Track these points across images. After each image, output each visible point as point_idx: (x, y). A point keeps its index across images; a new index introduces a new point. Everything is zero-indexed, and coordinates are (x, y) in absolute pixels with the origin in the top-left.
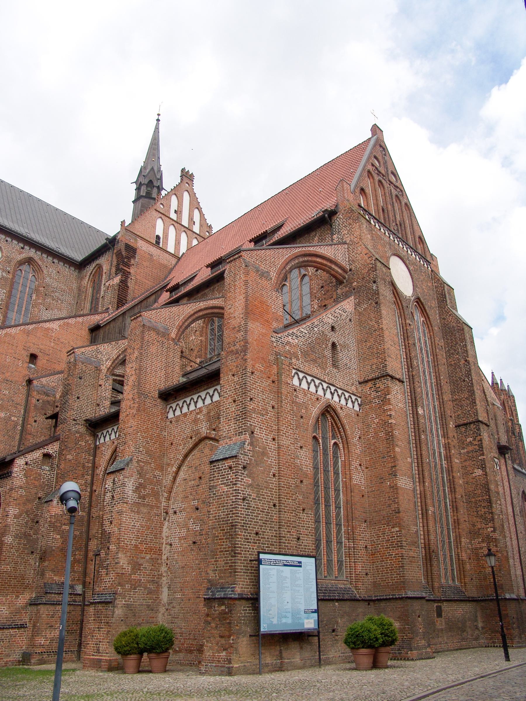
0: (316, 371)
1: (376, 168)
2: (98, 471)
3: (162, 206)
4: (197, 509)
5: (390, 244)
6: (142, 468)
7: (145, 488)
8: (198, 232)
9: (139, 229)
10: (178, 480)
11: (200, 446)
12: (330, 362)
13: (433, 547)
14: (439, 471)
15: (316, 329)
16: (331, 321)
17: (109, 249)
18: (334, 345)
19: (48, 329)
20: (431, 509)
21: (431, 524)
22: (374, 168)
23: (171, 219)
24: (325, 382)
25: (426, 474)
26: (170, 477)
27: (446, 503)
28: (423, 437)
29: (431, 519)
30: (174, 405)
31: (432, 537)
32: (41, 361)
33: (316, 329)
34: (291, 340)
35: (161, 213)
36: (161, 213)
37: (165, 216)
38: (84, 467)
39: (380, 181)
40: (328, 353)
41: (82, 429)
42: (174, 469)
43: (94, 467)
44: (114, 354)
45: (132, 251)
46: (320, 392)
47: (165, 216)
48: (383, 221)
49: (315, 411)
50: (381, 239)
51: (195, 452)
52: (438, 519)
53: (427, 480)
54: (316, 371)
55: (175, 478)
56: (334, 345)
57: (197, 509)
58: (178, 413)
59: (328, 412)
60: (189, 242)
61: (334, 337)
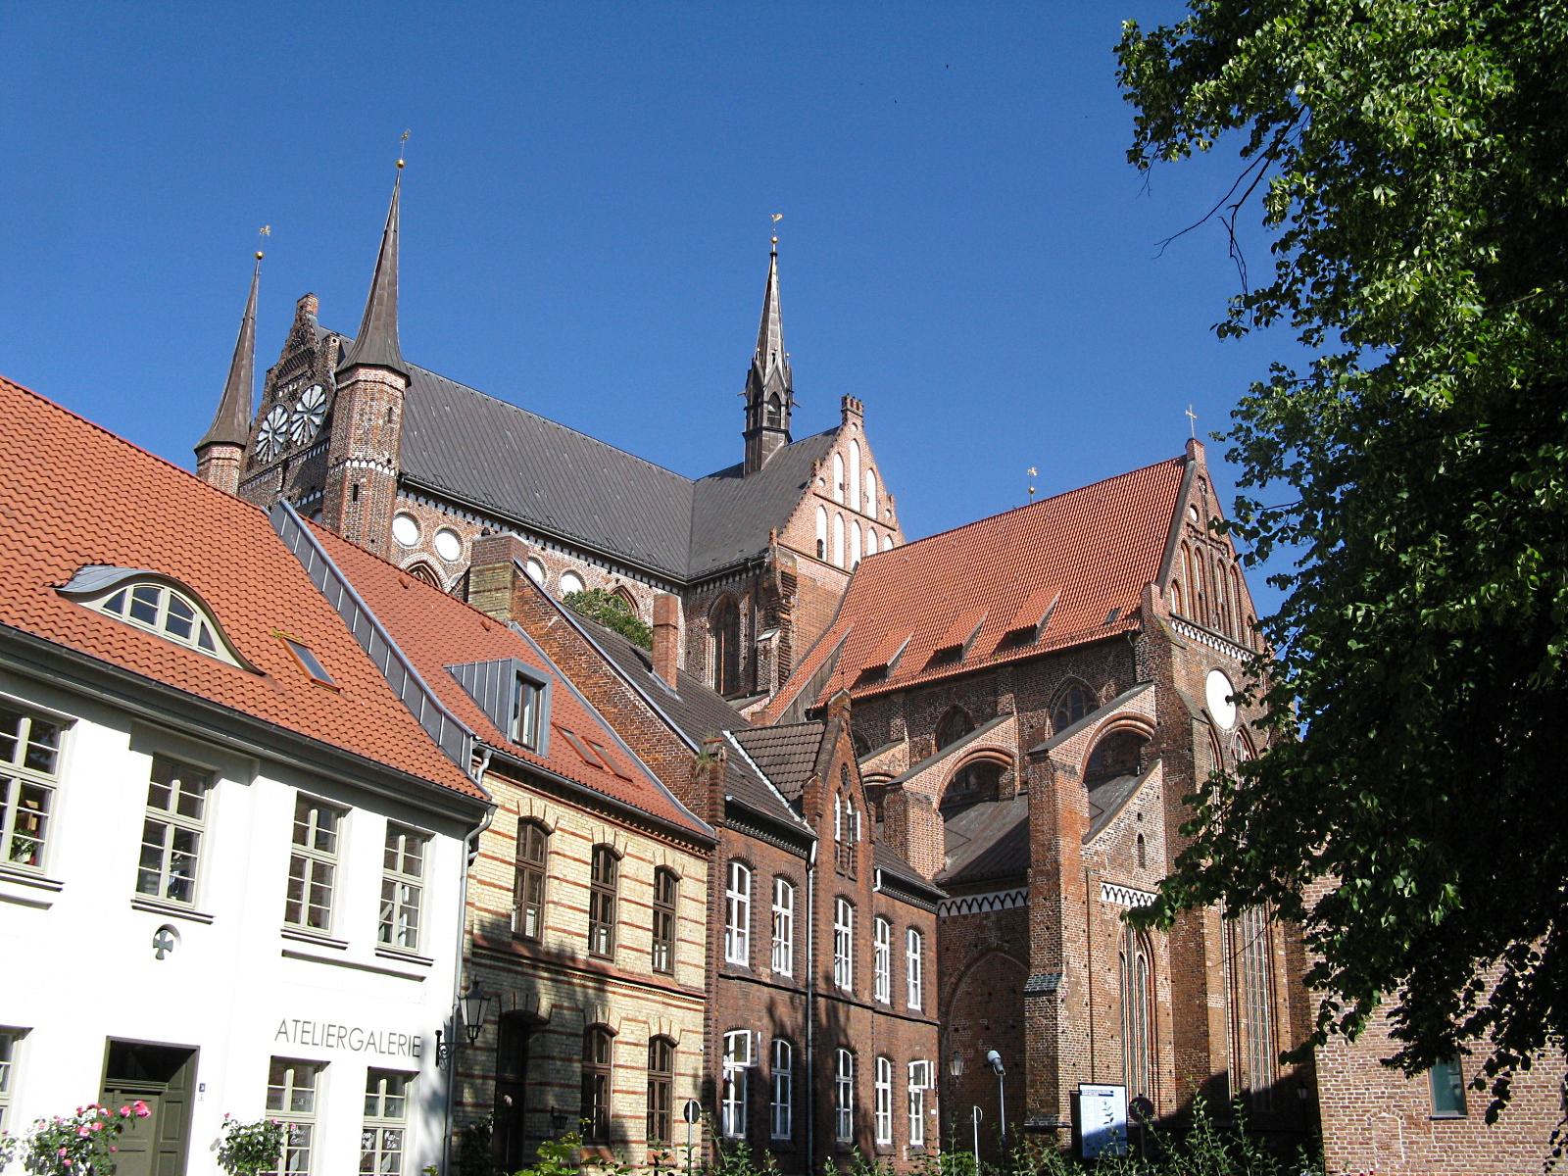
0: (1122, 878)
1: (1193, 527)
5: (1207, 656)
12: (1136, 862)
13: (1244, 1067)
14: (1257, 967)
18: (1140, 836)
20: (1243, 1021)
21: (1243, 1039)
22: (1190, 529)
25: (1240, 978)
27: (1263, 1010)
28: (1238, 930)
29: (1243, 1033)
31: (1244, 1056)
34: (1099, 848)
39: (1198, 549)
40: (1134, 851)
48: (1199, 624)
50: (1197, 653)
52: (1252, 1032)
53: (1241, 984)
54: (1122, 878)
56: (1140, 836)
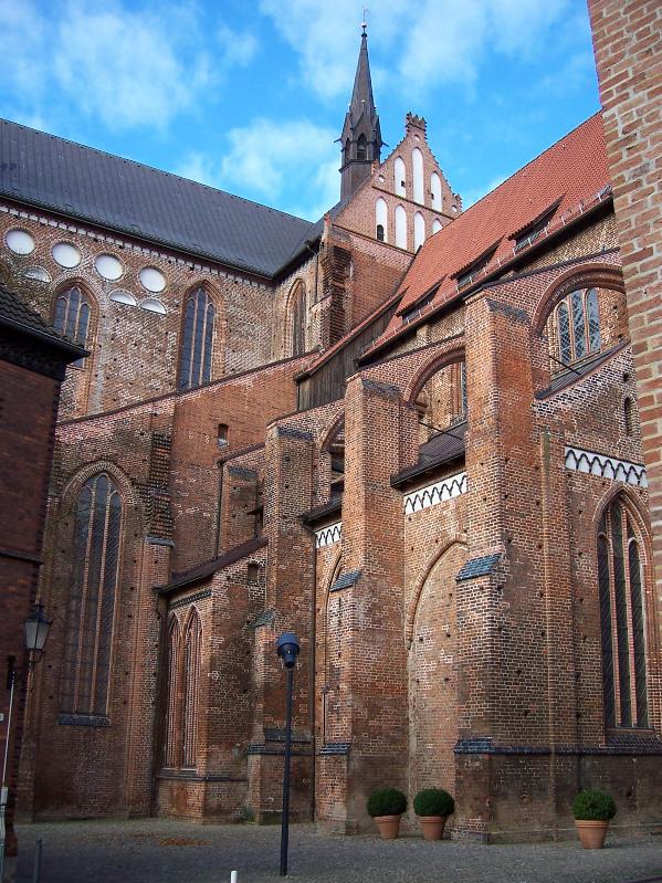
2: (320, 584)
3: (382, 180)
4: (449, 636)
6: (375, 583)
7: (380, 609)
8: (440, 210)
9: (350, 220)
10: (423, 596)
11: (449, 552)
12: (622, 427)
15: (599, 384)
16: (622, 368)
17: (311, 256)
18: (628, 401)
19: (240, 387)
23: (396, 196)
24: (615, 458)
26: (413, 594)
30: (412, 497)
32: (235, 433)
33: (599, 384)
35: (382, 191)
36: (382, 191)
37: (388, 193)
38: (301, 579)
40: (619, 415)
41: (297, 528)
42: (418, 583)
43: (315, 579)
44: (331, 420)
45: (342, 257)
46: (609, 474)
47: (388, 193)
49: (600, 502)
51: (443, 560)
54: (601, 444)
55: (419, 595)
56: (628, 401)
57: (449, 636)
58: (418, 507)
59: (622, 500)
60: (428, 228)
61: (625, 390)
